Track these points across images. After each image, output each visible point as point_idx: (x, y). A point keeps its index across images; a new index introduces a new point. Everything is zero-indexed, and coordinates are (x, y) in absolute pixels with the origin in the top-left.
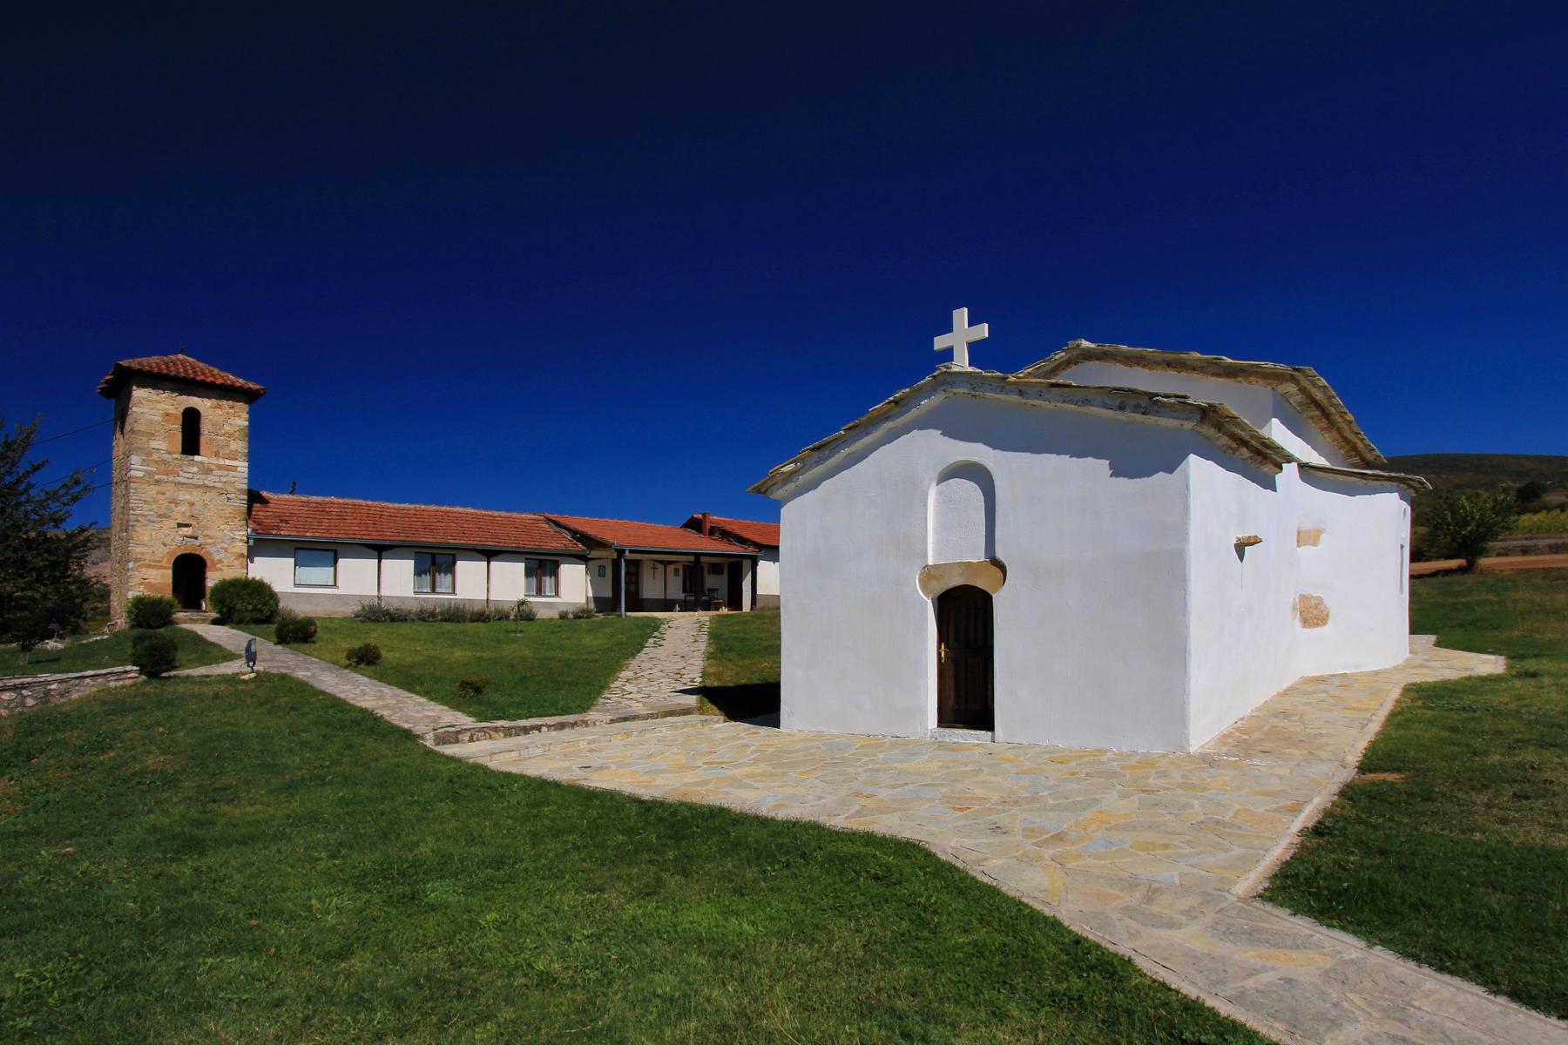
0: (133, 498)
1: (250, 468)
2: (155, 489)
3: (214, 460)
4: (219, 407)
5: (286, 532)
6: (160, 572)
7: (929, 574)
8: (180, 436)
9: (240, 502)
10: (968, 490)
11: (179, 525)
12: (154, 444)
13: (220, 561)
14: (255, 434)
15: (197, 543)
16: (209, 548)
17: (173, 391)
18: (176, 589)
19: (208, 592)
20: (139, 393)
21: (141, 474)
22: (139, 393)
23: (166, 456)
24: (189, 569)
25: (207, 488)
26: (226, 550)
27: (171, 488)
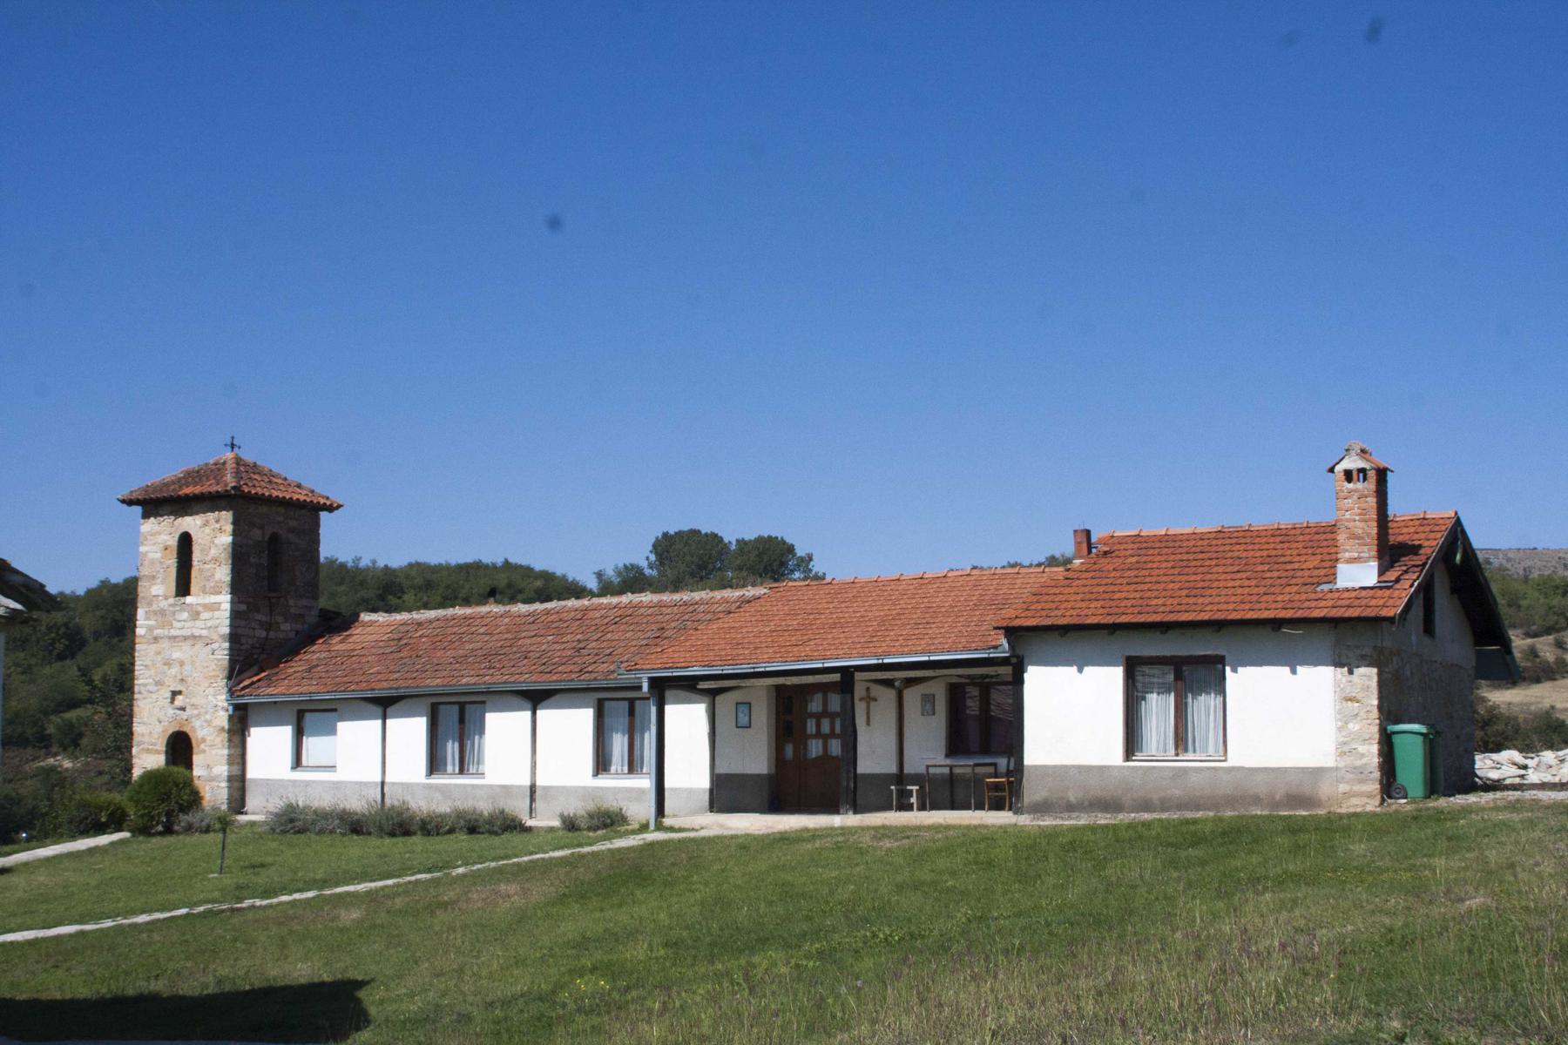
2: (154, 647)
13: (204, 740)
15: (184, 715)
16: (197, 723)
17: (169, 514)
23: (164, 604)
26: (209, 723)
27: (165, 644)
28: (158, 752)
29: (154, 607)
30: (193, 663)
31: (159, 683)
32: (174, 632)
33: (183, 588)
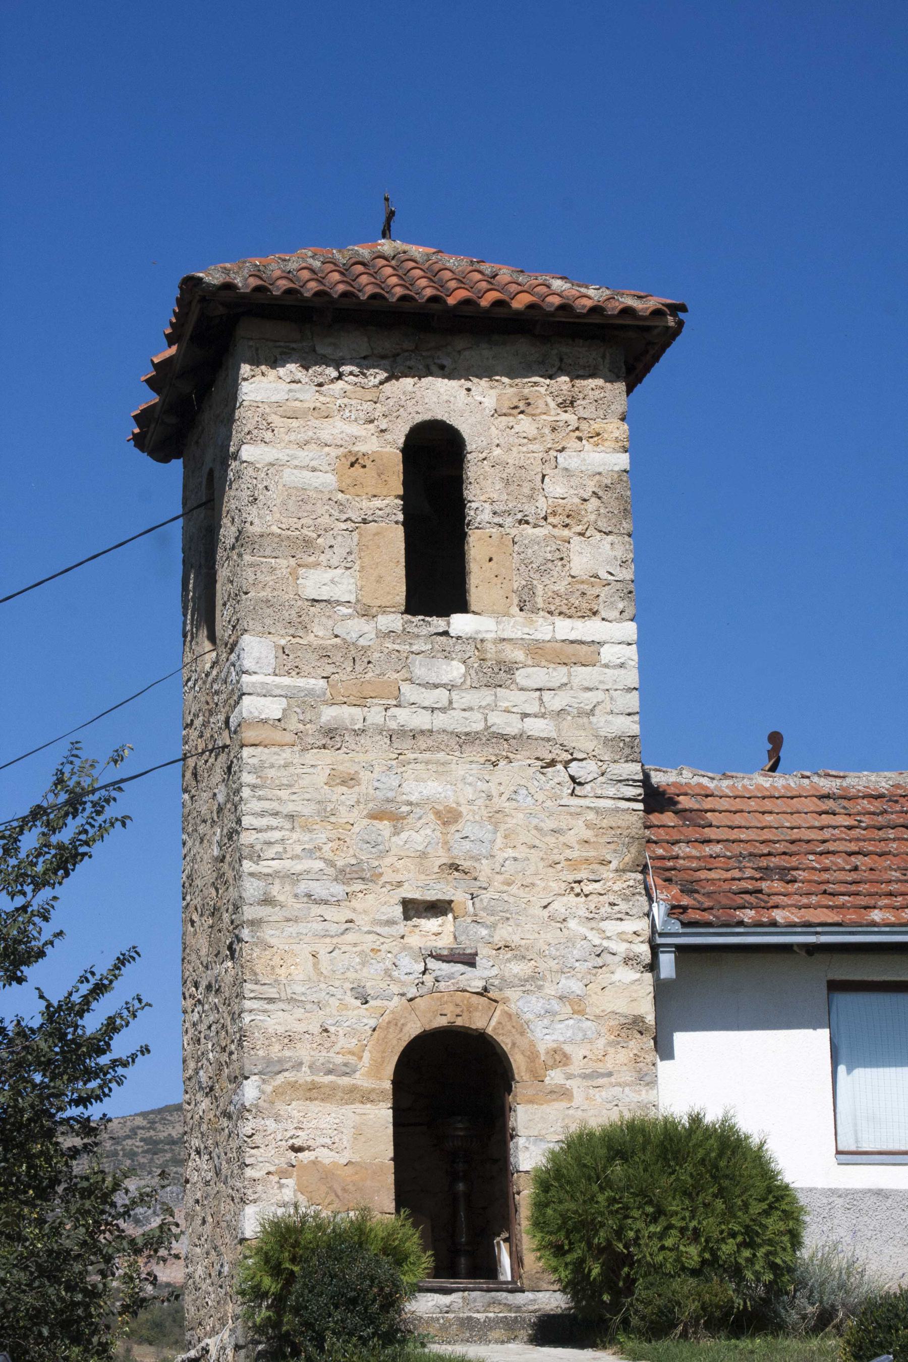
0: (251, 804)
1: (642, 643)
3: (516, 627)
4: (523, 407)
5: (792, 916)
6: (348, 1115)
8: (400, 531)
11: (413, 909)
12: (316, 582)
13: (559, 1057)
14: (645, 503)
16: (526, 1006)
17: (365, 362)
18: (404, 1196)
19: (525, 1196)
20: (262, 388)
21: (273, 708)
22: (262, 388)
23: (357, 629)
24: (451, 1087)
25: (499, 745)
27: (376, 752)
28: (366, 1097)
29: (319, 632)
30: (496, 817)
31: (357, 875)
32: (404, 717)
33: (436, 578)
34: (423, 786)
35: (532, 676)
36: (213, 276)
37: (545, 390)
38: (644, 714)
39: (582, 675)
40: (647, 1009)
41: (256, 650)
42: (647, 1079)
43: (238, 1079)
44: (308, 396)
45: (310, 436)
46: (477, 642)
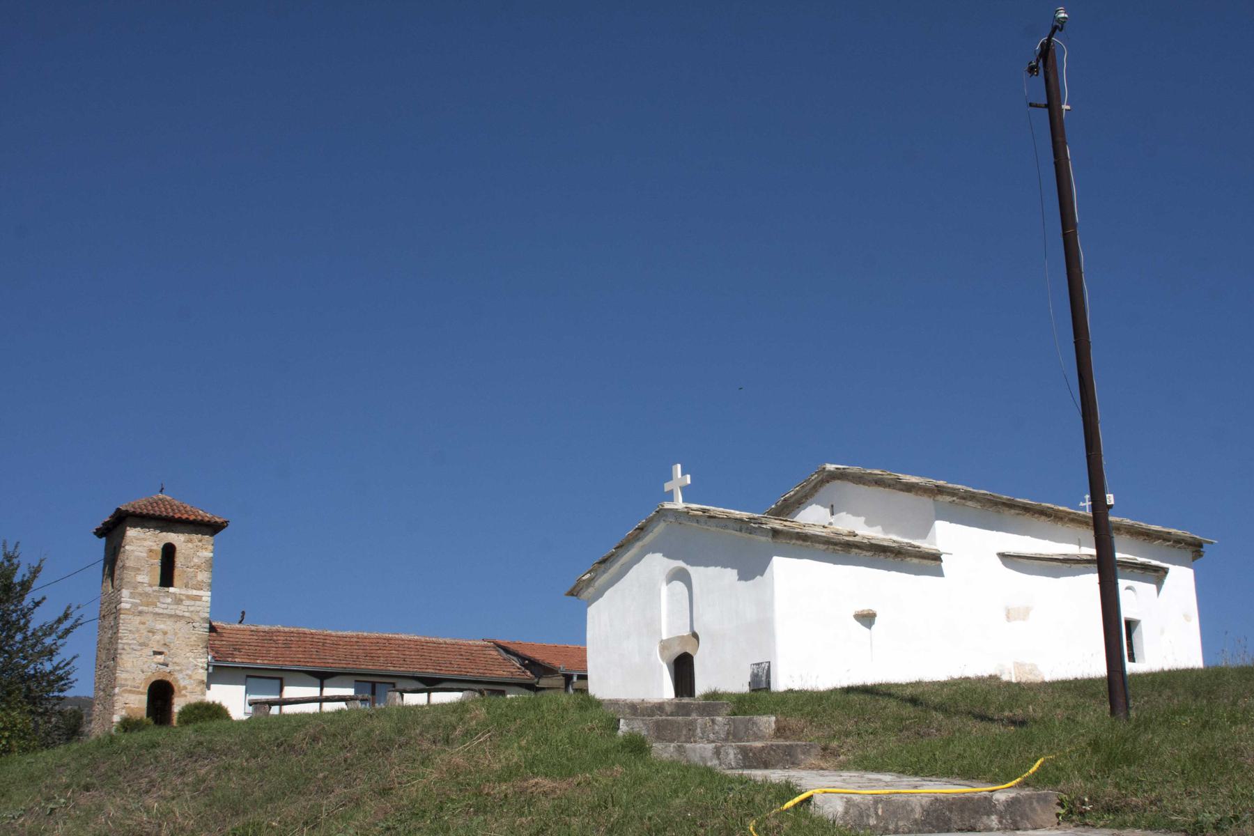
0: (122, 627)
1: (212, 597)
2: (138, 619)
3: (184, 591)
4: (190, 541)
5: (239, 660)
6: (138, 697)
7: (665, 646)
9: (203, 630)
10: (679, 586)
11: (156, 653)
12: (140, 578)
13: (185, 688)
16: (179, 676)
17: (155, 528)
19: (175, 718)
20: (132, 533)
21: (127, 606)
22: (132, 533)
23: (148, 589)
24: (161, 693)
25: (177, 618)
26: (190, 677)
29: (140, 590)
30: (176, 634)
31: (143, 645)
32: (157, 610)
33: (167, 579)
34: (160, 626)
35: (187, 602)
36: (123, 508)
37: (195, 537)
38: (210, 613)
39: (198, 603)
40: (205, 678)
41: (125, 593)
42: (204, 694)
43: (114, 688)
44: (142, 535)
45: (141, 544)
46: (174, 594)
